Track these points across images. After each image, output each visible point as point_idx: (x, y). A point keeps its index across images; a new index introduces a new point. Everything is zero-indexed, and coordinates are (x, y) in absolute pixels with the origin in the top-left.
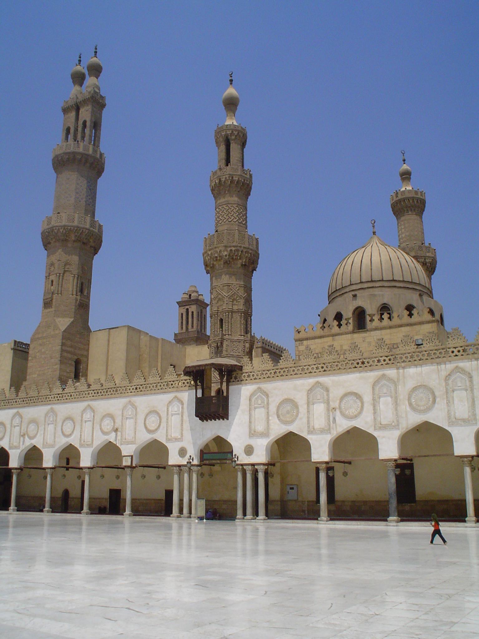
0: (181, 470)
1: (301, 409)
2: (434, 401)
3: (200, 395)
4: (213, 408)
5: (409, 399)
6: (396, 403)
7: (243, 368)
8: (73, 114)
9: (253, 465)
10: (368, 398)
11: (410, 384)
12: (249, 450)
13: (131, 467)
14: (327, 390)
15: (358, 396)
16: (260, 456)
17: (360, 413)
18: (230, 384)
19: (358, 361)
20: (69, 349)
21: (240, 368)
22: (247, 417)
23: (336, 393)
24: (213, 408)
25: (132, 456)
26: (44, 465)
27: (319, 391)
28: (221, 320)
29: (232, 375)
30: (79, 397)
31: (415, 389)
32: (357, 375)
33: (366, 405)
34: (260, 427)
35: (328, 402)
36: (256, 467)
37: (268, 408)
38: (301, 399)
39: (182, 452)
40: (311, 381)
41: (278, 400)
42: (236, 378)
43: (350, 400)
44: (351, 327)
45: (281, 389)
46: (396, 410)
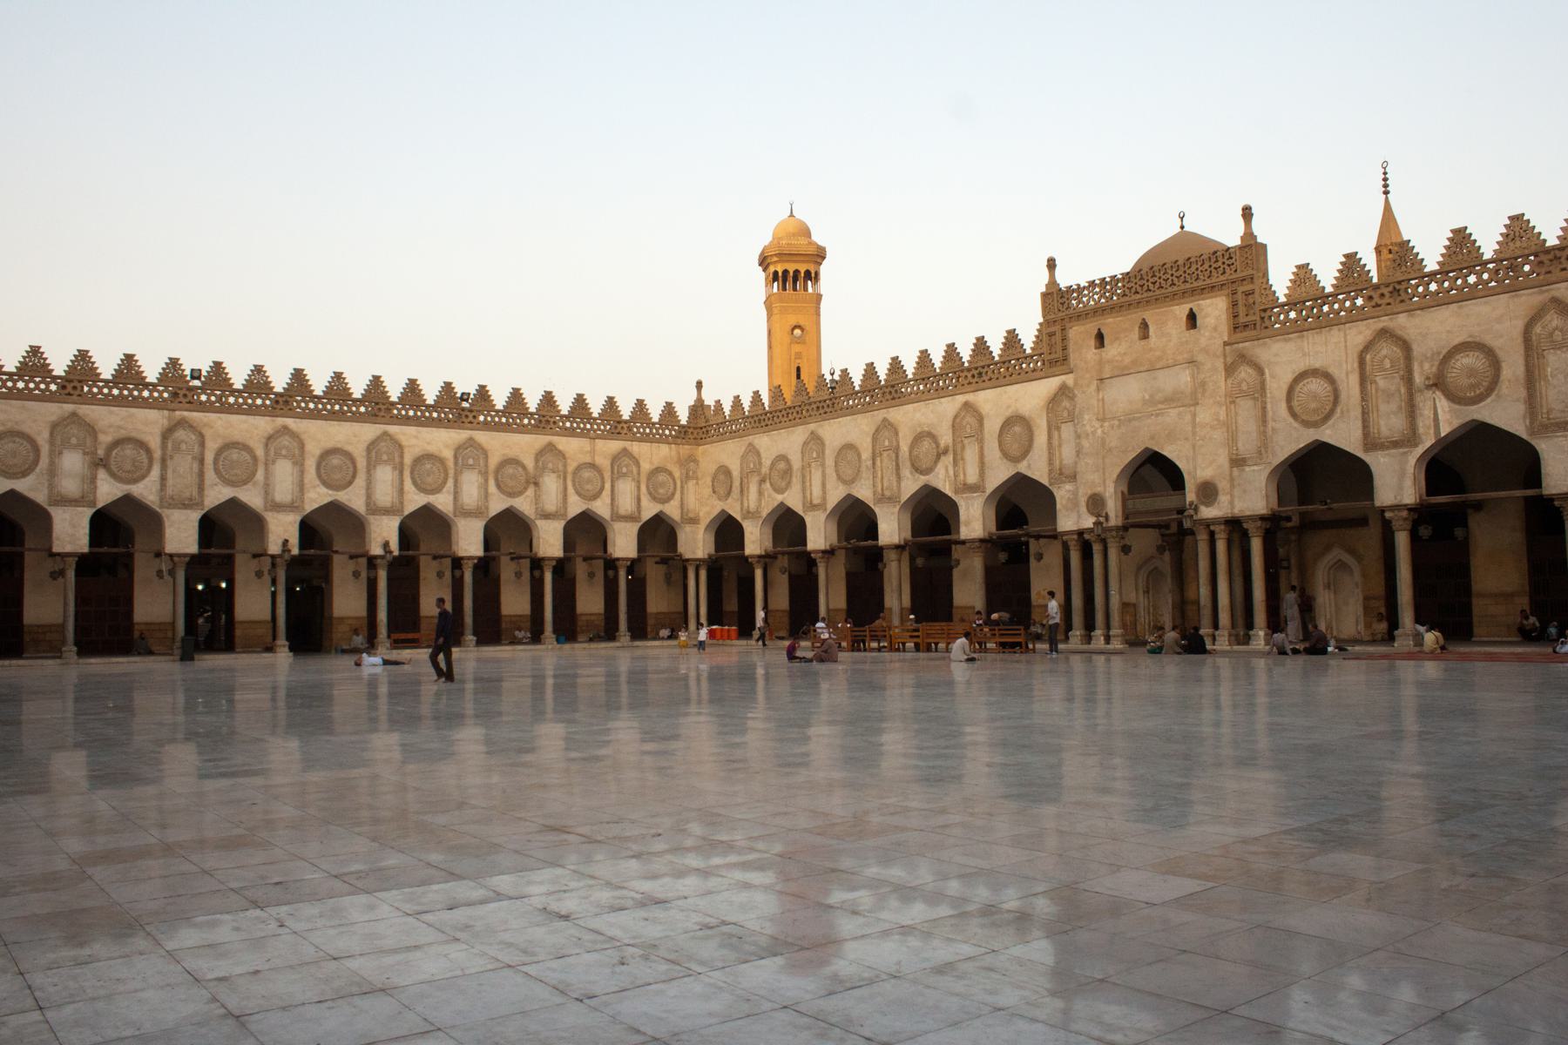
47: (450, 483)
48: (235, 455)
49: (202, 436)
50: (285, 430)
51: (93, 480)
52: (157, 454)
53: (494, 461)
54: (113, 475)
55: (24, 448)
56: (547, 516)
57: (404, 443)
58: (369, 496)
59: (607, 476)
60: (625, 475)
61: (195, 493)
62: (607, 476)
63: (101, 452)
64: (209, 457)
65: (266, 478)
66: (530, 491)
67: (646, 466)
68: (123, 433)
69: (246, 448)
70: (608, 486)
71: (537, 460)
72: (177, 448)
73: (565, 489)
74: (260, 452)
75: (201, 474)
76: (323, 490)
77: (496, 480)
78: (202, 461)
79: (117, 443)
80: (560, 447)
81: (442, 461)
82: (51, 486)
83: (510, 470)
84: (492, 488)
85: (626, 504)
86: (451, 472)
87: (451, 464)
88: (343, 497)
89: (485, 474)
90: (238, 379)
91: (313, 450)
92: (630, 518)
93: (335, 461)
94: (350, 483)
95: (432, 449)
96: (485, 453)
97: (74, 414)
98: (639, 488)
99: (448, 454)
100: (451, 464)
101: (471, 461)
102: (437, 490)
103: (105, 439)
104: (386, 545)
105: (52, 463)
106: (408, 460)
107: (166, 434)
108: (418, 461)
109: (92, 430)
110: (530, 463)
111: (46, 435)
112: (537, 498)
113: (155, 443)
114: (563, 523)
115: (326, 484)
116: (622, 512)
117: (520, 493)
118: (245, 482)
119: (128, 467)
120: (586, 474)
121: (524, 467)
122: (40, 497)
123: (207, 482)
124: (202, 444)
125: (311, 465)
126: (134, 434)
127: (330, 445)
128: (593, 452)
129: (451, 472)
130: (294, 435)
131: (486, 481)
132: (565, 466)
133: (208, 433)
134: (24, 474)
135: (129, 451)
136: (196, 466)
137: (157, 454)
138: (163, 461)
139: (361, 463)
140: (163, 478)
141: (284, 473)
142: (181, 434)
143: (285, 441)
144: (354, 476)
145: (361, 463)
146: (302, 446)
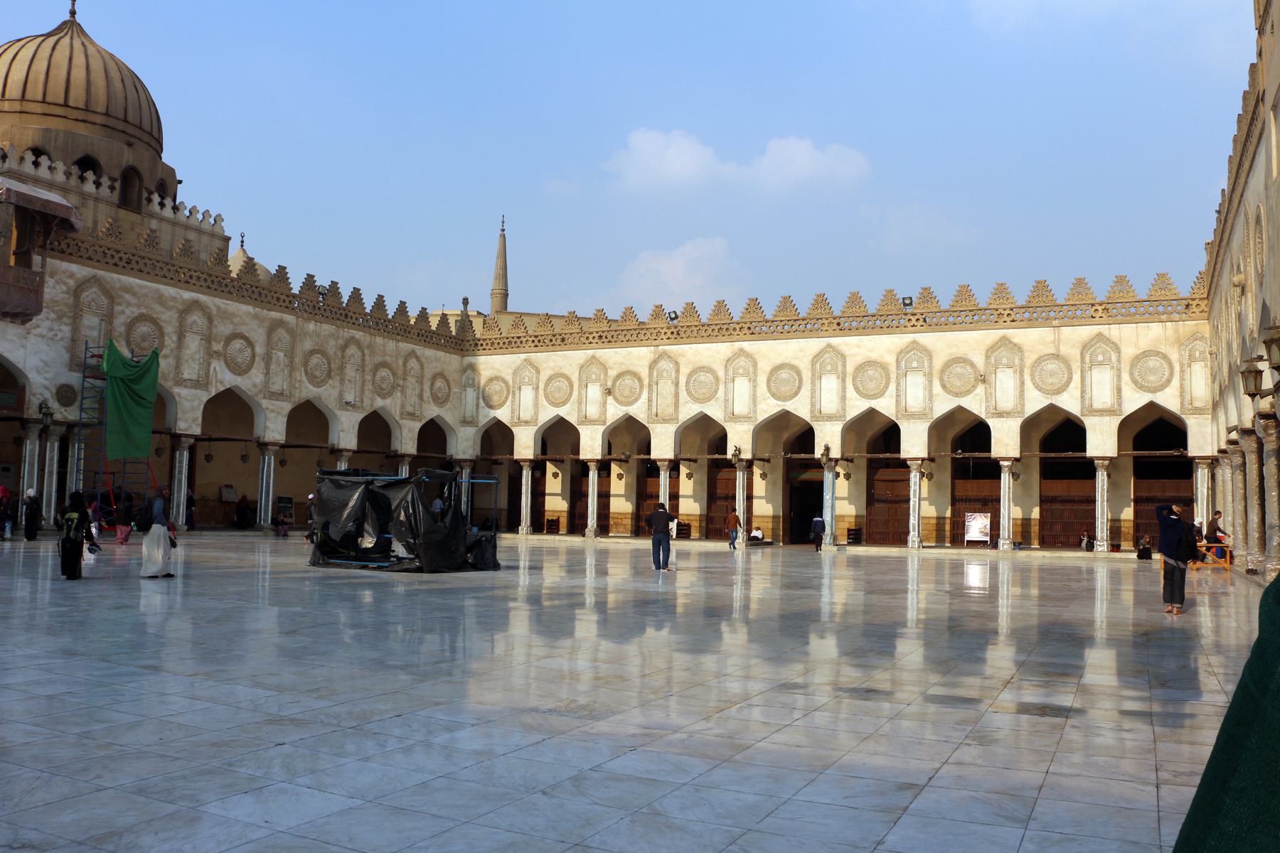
1: (168, 341)
2: (329, 376)
5: (305, 364)
6: (292, 367)
10: (259, 350)
11: (308, 345)
14: (210, 320)
15: (250, 344)
17: (249, 368)
22: (66, 330)
23: (223, 329)
27: (195, 318)
31: (312, 352)
32: (250, 309)
33: (257, 359)
35: (208, 339)
37: (111, 323)
38: (168, 319)
40: (188, 295)
41: (132, 312)
43: (237, 344)
46: (290, 375)
47: (892, 387)
48: (703, 377)
49: (677, 363)
50: (742, 352)
51: (604, 404)
52: (646, 382)
53: (938, 363)
54: (616, 400)
55: (564, 384)
56: (1000, 415)
57: (847, 353)
58: (813, 405)
59: (1076, 366)
60: (1101, 364)
61: (671, 410)
62: (1076, 366)
63: (609, 384)
64: (683, 380)
65: (726, 395)
66: (980, 389)
67: (1129, 352)
68: (624, 368)
69: (710, 370)
70: (1077, 377)
71: (987, 357)
72: (660, 376)
73: (1022, 383)
74: (721, 374)
75: (677, 395)
76: (773, 401)
77: (941, 380)
78: (677, 384)
79: (619, 376)
80: (1016, 340)
81: (884, 367)
82: (579, 411)
83: (958, 369)
84: (937, 387)
85: (1102, 395)
86: (893, 376)
87: (893, 368)
88: (790, 406)
89: (929, 376)
90: (705, 314)
91: (765, 367)
92: (1109, 412)
93: (784, 374)
94: (796, 394)
95: (874, 356)
96: (929, 354)
97: (593, 357)
98: (1119, 376)
99: (890, 359)
100: (893, 368)
101: (915, 364)
102: (880, 394)
103: (612, 373)
104: (827, 449)
105: (580, 393)
106: (850, 368)
107: (653, 365)
108: (861, 368)
109: (605, 368)
110: (979, 361)
111: (577, 374)
112: (988, 396)
113: (644, 373)
114: (1019, 421)
115: (773, 395)
116: (1097, 405)
117: (969, 392)
118: (709, 399)
119: (626, 393)
120: (1051, 366)
121: (972, 365)
122: (572, 419)
123: (681, 401)
124: (678, 371)
125: (762, 380)
126: (631, 368)
127: (779, 362)
128: (1057, 342)
129: (893, 376)
130: (749, 356)
131: (930, 382)
132: (1022, 360)
133: (681, 361)
134: (564, 403)
135: (628, 381)
136: (673, 388)
137: (646, 382)
138: (650, 386)
139: (807, 376)
140: (650, 400)
141: (742, 387)
142: (664, 364)
143: (742, 361)
144: (799, 388)
145: (807, 376)
146: (755, 365)
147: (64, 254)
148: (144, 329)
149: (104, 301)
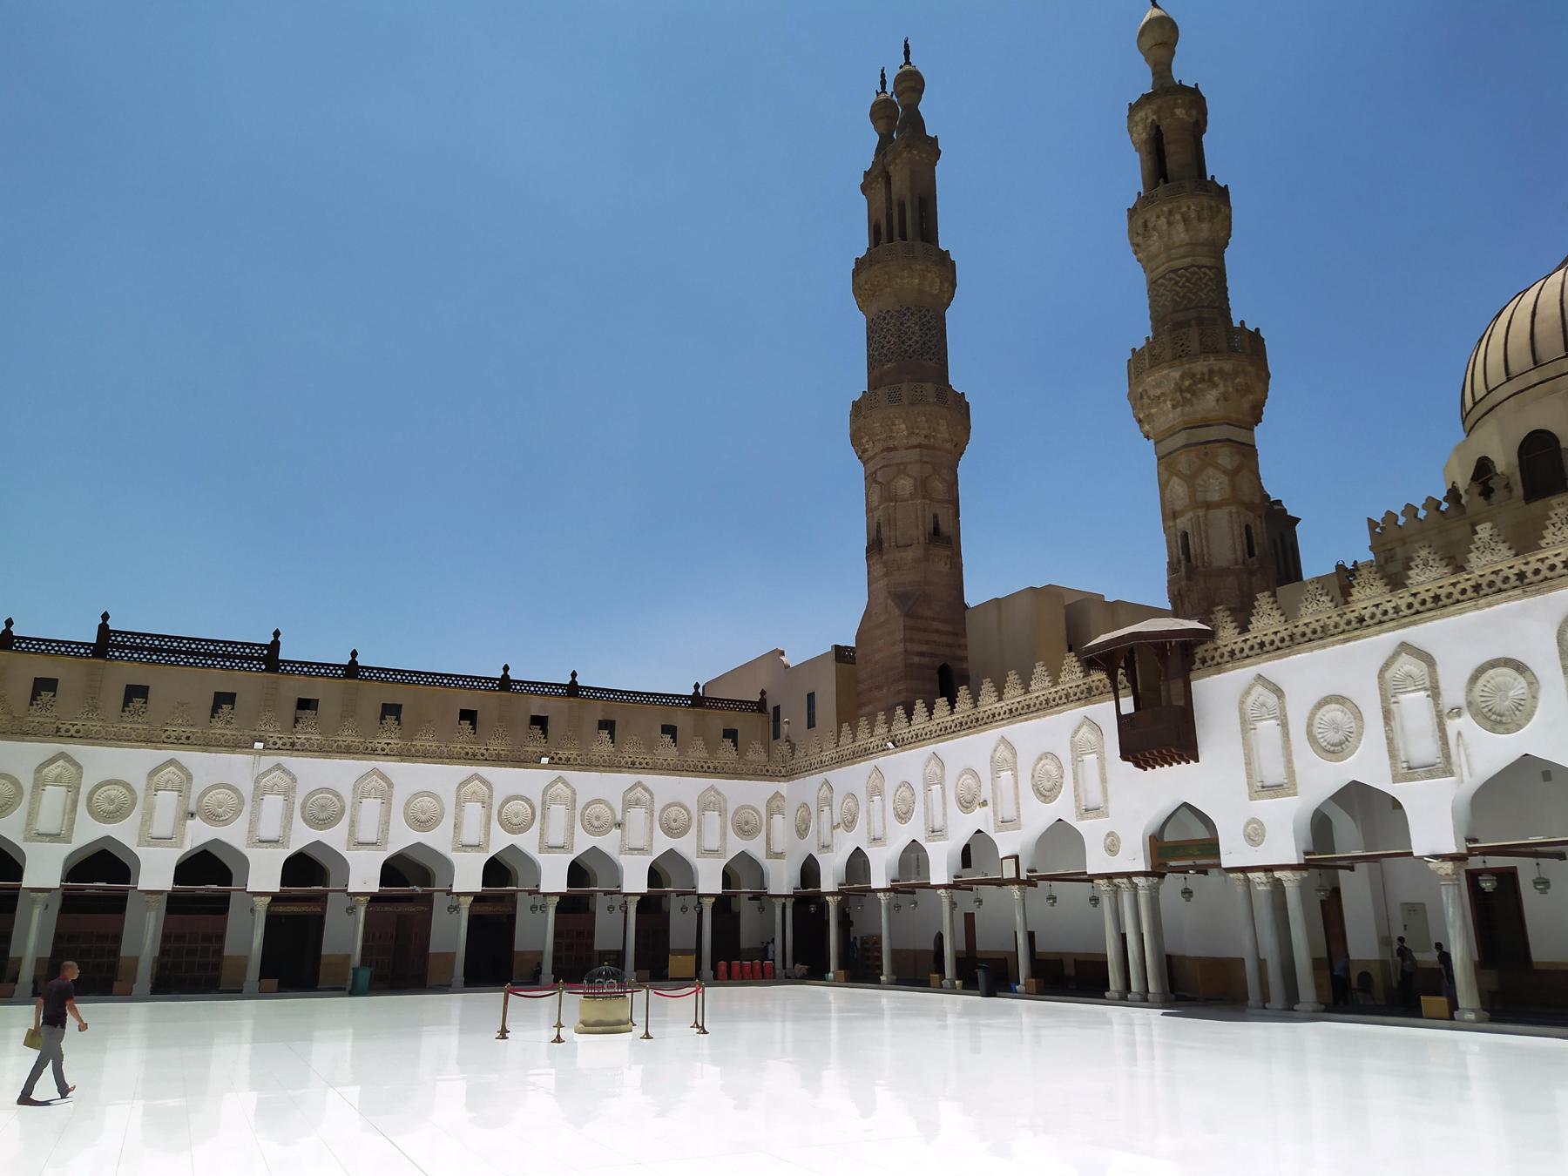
0: (1118, 886)
3: (1128, 705)
4: (1161, 735)
7: (1221, 633)
8: (880, 187)
9: (1268, 869)
12: (1255, 834)
13: (1017, 881)
16: (1284, 847)
18: (1192, 675)
19: (1507, 572)
20: (924, 648)
21: (1210, 636)
24: (1161, 735)
25: (1017, 857)
26: (873, 886)
28: (1185, 535)
29: (1193, 655)
30: (919, 739)
34: (1273, 772)
35: (1435, 692)
36: (1277, 874)
39: (1112, 846)
42: (1204, 661)
44: (1519, 490)
45: (1306, 674)
147: (1218, 667)
148: (1333, 712)
149: (1271, 699)
